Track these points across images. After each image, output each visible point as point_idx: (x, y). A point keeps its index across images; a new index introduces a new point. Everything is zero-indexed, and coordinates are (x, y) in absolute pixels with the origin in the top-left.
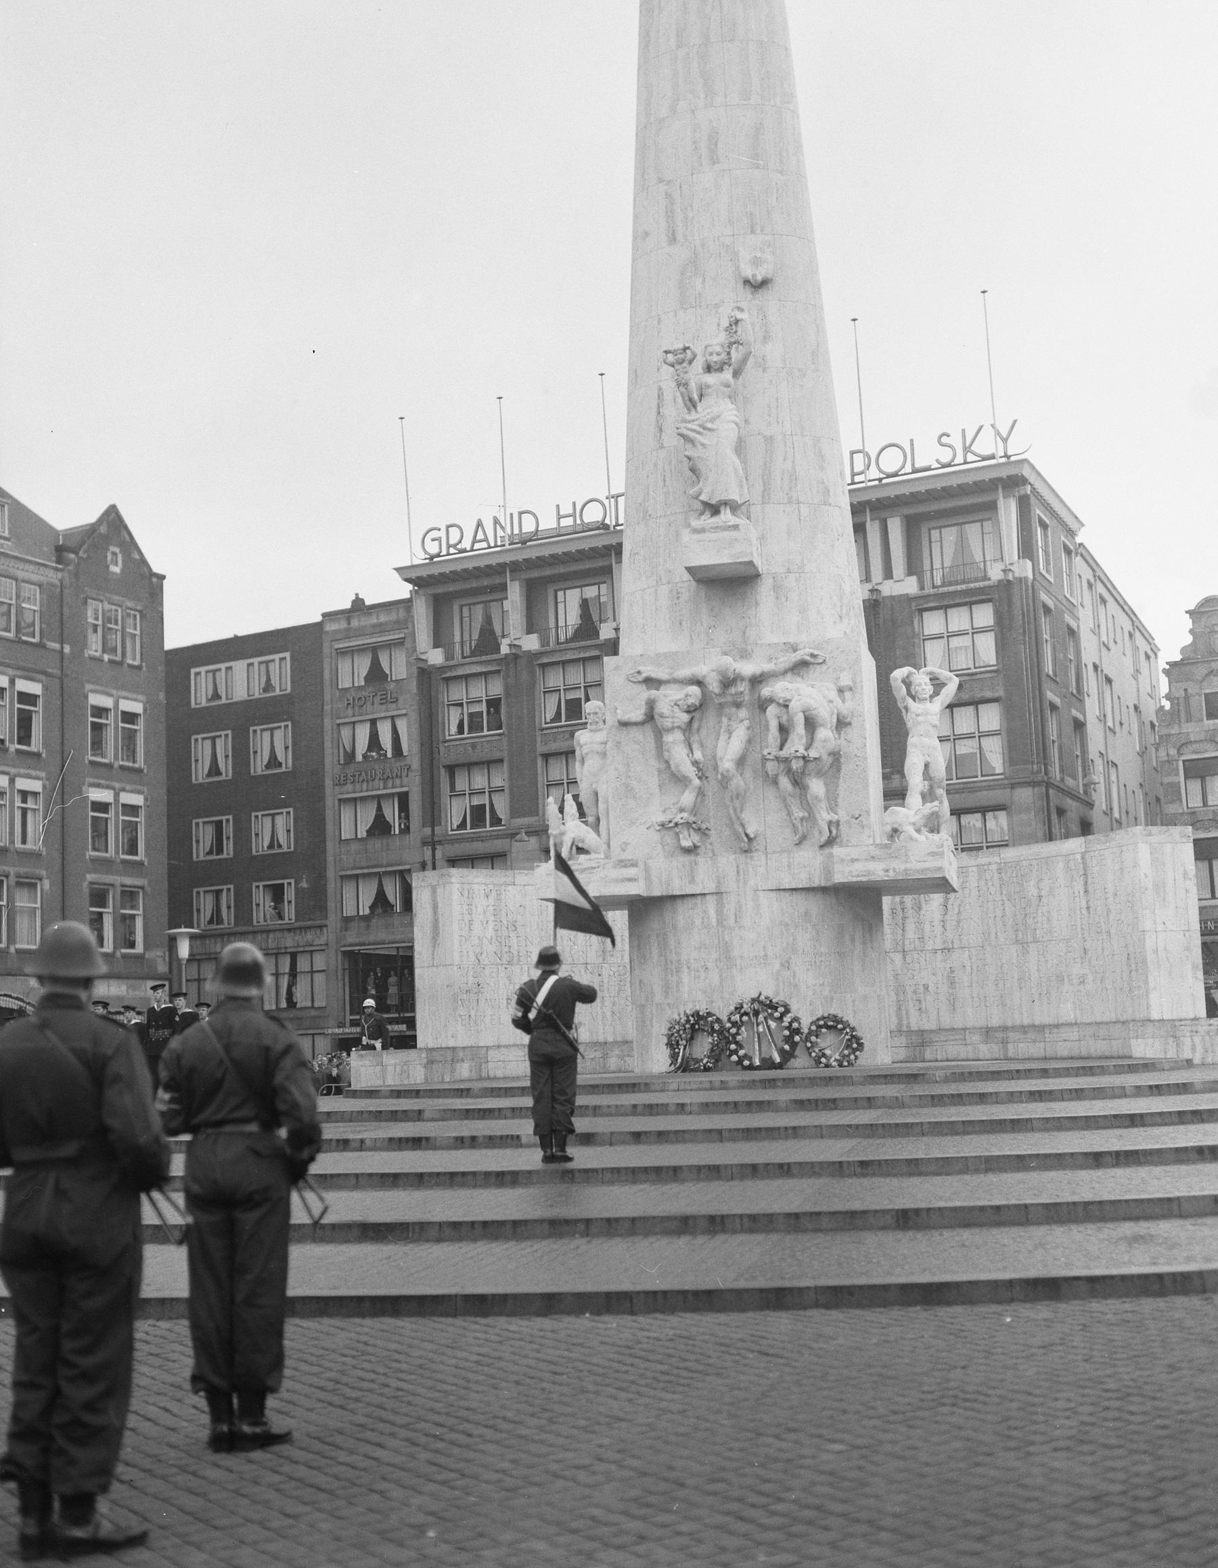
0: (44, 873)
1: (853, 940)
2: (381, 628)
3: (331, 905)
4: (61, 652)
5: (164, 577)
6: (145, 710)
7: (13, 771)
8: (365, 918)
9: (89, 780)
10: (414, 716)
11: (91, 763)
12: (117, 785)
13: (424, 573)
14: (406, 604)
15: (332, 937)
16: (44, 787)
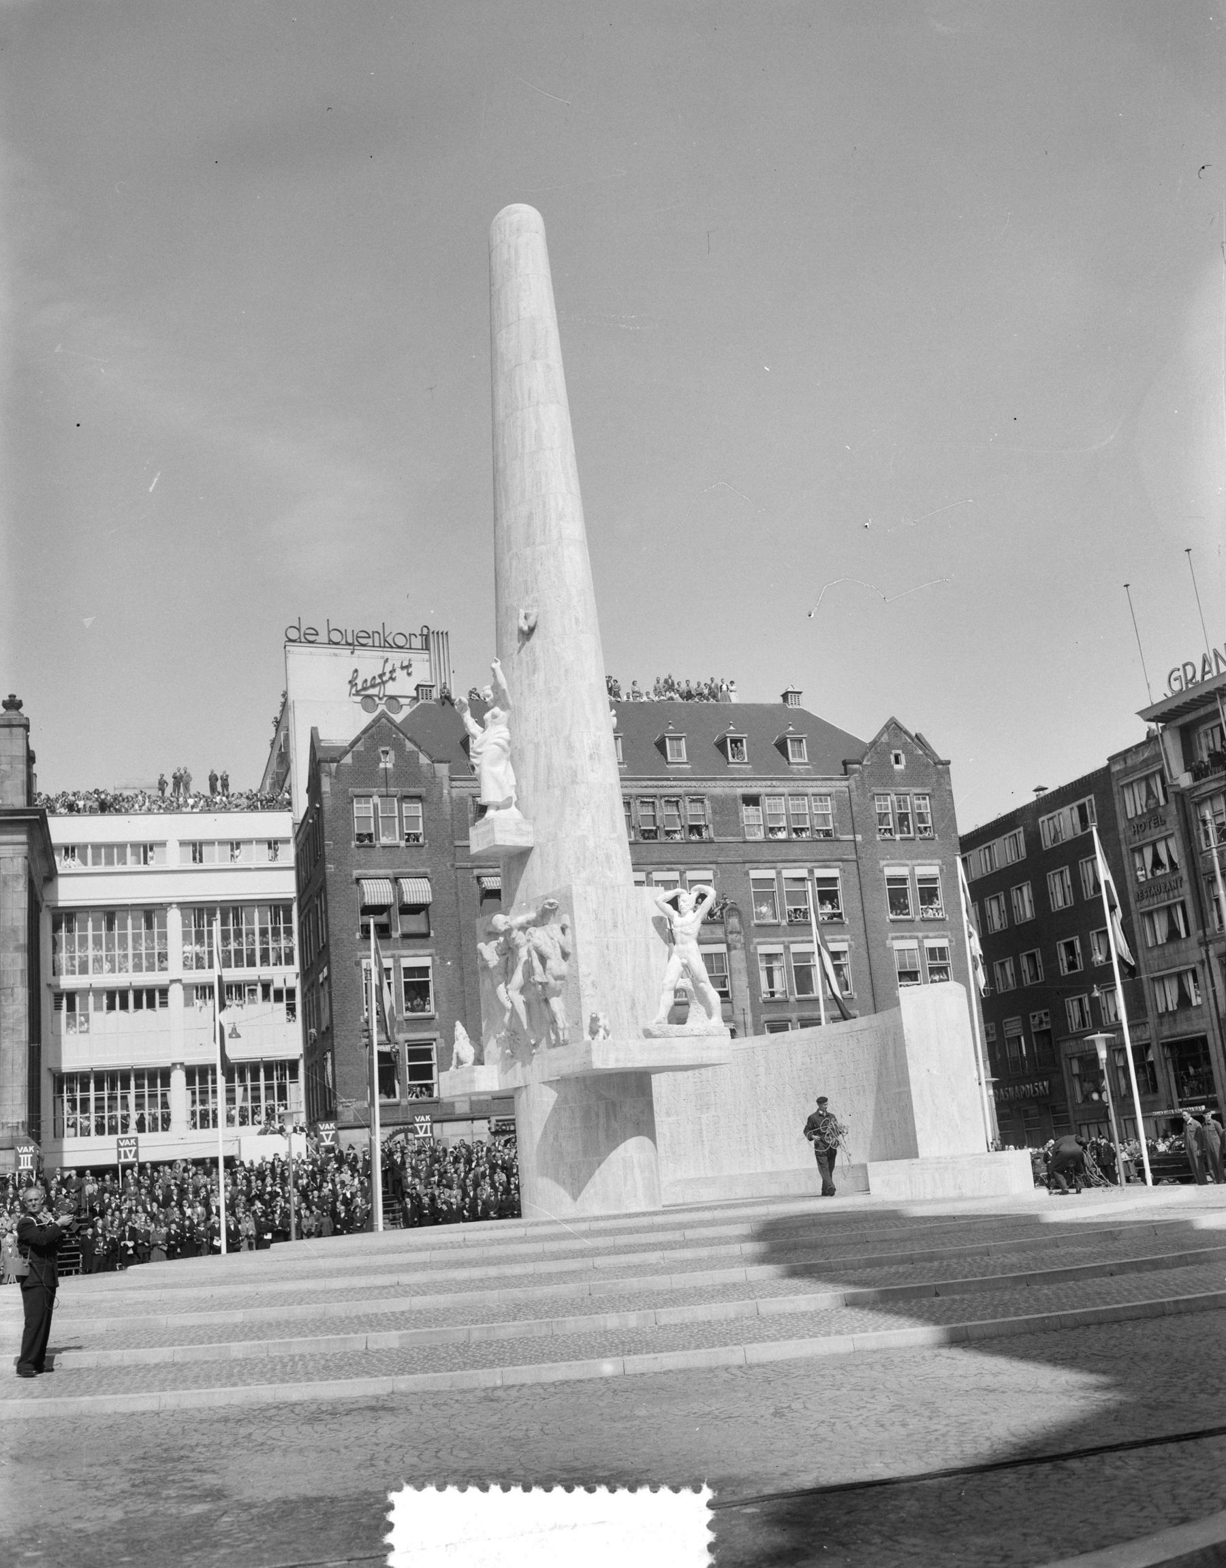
1: (598, 1115)
2: (1146, 763)
3: (1148, 1004)
5: (948, 763)
6: (941, 870)
8: (1173, 1013)
9: (890, 935)
10: (1177, 834)
11: (893, 921)
12: (920, 935)
13: (1158, 712)
14: (1152, 739)
15: (1153, 1032)
16: (850, 946)
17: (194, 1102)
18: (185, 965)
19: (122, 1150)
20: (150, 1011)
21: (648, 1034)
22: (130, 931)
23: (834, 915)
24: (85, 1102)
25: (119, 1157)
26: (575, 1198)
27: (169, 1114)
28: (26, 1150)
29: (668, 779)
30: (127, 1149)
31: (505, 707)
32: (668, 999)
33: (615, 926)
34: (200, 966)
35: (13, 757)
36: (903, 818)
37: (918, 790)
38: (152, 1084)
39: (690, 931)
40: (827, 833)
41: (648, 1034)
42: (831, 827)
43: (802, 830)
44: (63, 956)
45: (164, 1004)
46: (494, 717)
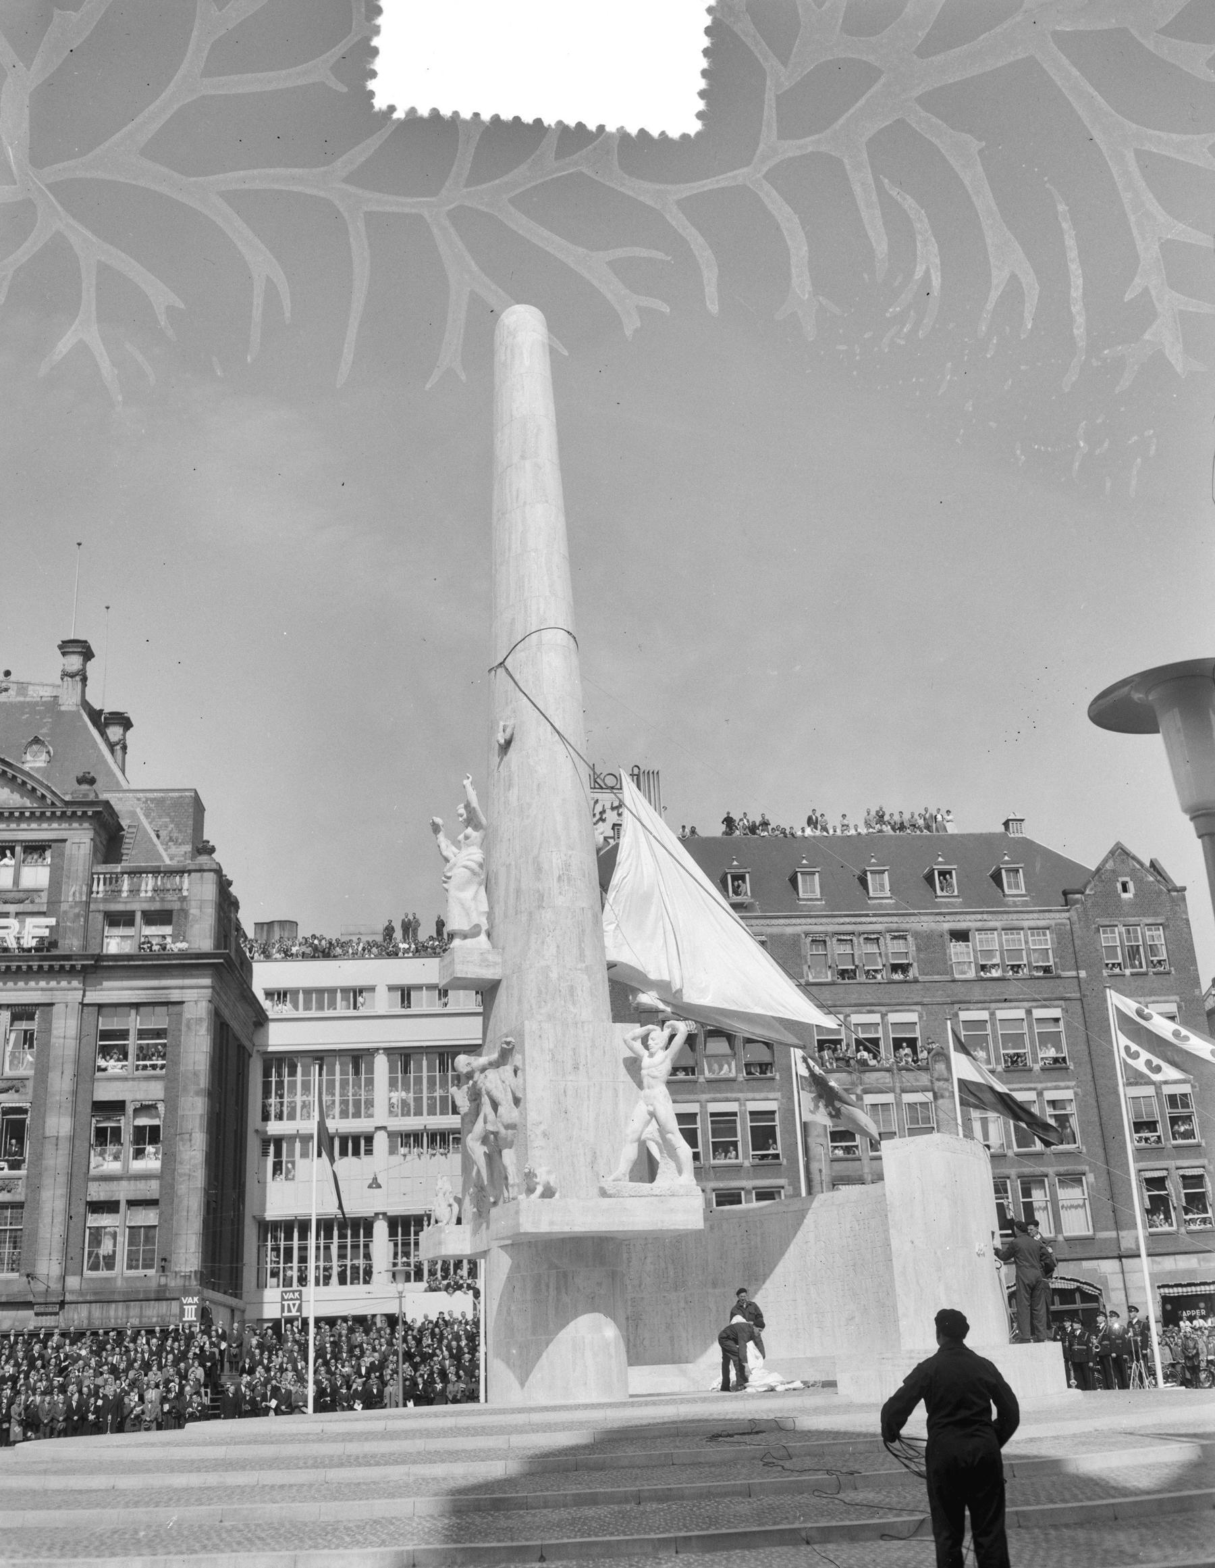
0: (1087, 1168)
4: (1078, 977)
7: (1039, 1086)
16: (1076, 1094)
17: (396, 1255)
18: (391, 1112)
19: (286, 1303)
20: (355, 1159)
21: (603, 1193)
22: (338, 1077)
23: (1056, 1060)
24: (288, 1251)
25: (283, 1311)
26: (522, 1384)
27: (371, 1267)
28: (190, 1300)
29: (867, 915)
30: (291, 1303)
31: (478, 827)
32: (630, 1153)
33: (576, 1068)
34: (406, 1113)
35: (202, 901)
36: (1133, 952)
37: (1149, 921)
38: (355, 1235)
39: (656, 1074)
40: (1047, 970)
41: (603, 1193)
42: (1051, 963)
43: (1019, 966)
44: (273, 1100)
45: (369, 1152)
46: (467, 838)
